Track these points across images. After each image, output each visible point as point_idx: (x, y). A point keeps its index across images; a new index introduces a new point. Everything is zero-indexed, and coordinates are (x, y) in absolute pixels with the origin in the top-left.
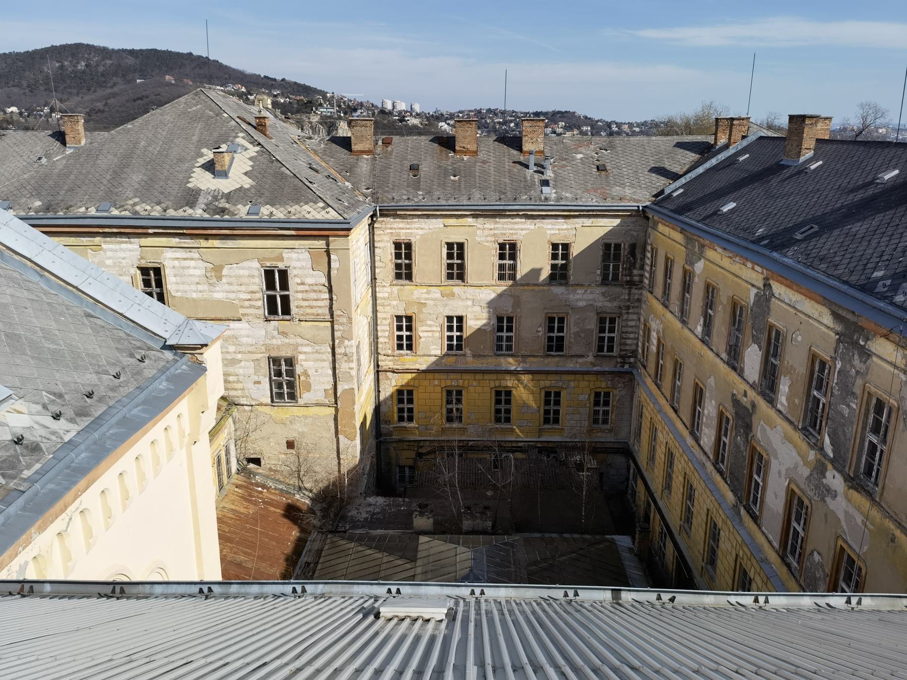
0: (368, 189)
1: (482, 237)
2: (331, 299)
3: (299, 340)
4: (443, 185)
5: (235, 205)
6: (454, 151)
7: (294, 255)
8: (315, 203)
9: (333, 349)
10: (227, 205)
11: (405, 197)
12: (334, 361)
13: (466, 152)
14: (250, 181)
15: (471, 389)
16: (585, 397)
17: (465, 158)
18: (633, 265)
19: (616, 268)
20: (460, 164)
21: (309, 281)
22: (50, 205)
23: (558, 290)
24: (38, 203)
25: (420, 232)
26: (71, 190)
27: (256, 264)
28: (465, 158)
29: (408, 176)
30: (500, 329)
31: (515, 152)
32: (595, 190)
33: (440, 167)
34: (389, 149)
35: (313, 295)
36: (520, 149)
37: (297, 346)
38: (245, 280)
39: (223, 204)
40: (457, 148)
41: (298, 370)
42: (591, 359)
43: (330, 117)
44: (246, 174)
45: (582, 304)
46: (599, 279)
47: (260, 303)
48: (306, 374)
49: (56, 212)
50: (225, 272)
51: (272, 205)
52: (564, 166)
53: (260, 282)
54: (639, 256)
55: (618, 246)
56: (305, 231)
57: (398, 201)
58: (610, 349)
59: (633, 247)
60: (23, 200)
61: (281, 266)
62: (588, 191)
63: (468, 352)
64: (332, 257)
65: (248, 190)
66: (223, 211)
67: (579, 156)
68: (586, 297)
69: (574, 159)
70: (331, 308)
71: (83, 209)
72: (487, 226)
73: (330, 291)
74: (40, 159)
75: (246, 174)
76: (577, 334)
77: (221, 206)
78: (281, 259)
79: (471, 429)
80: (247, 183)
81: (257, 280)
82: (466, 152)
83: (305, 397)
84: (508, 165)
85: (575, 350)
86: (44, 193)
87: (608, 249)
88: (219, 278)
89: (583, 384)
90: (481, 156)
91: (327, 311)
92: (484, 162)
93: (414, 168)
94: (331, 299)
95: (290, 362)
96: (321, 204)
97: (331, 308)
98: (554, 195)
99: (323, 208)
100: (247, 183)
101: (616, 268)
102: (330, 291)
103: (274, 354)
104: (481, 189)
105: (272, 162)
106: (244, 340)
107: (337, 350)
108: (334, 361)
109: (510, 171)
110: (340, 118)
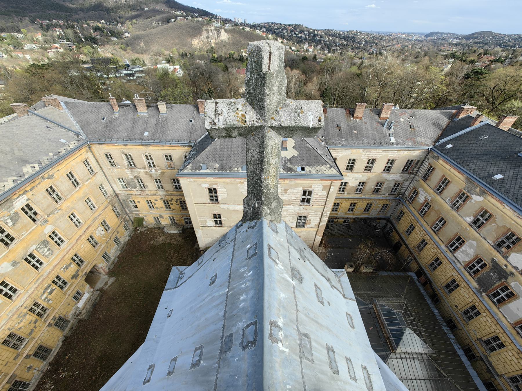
0: (322, 137)
1: (362, 155)
2: (326, 200)
3: (310, 211)
4: (351, 135)
5: (294, 166)
6: (353, 117)
7: (317, 186)
8: (326, 165)
9: (322, 213)
10: (291, 166)
11: (338, 142)
12: (321, 217)
13: (357, 118)
14: (296, 152)
15: (343, 203)
16: (380, 205)
17: (358, 120)
18: (415, 167)
19: (408, 167)
20: (356, 124)
21: (320, 194)
22: (222, 167)
23: (385, 175)
24: (217, 166)
25: (341, 155)
26: (228, 158)
27: (301, 189)
28: (358, 120)
29: (336, 130)
30: (359, 185)
31: (377, 117)
32: (411, 139)
33: (348, 125)
34: (327, 115)
35: (320, 198)
36: (379, 117)
37: (308, 213)
38: (296, 194)
39: (290, 166)
40: (355, 116)
41: (308, 219)
42: (387, 195)
43: (218, 27)
44: (293, 147)
45: (391, 179)
46: (401, 171)
47: (299, 200)
48: (310, 220)
49: (226, 171)
50: (288, 191)
51: (309, 166)
52: (397, 126)
53: (301, 194)
54: (419, 164)
55: (412, 161)
56: (322, 177)
57: (335, 145)
58: (394, 192)
59: (419, 161)
60: (211, 163)
61: (310, 189)
62: (408, 139)
63: (346, 192)
64: (332, 187)
65: (297, 157)
66: (290, 170)
67: (402, 120)
68: (394, 176)
69: (400, 122)
70: (326, 202)
71: (236, 169)
72: (367, 153)
73: (327, 197)
74: (191, 121)
75: (293, 147)
76: (385, 188)
77: (289, 166)
78: (311, 187)
79: (339, 213)
80: (296, 153)
81: (300, 194)
82: (357, 118)
83: (308, 226)
84: (375, 125)
85: (383, 192)
86: (218, 160)
87: (410, 162)
88: (286, 193)
89: (381, 202)
90: (364, 119)
91: (324, 203)
92: (365, 123)
93: (338, 126)
94: (326, 200)
95: (305, 217)
96: (328, 166)
97: (326, 202)
98: (395, 142)
99: (330, 168)
100: (296, 153)
101: (408, 167)
102: (327, 197)
103: (300, 215)
104: (367, 138)
105: (302, 140)
106: (290, 211)
107: (324, 214)
108: (321, 217)
109: (376, 128)
110: (221, 28)
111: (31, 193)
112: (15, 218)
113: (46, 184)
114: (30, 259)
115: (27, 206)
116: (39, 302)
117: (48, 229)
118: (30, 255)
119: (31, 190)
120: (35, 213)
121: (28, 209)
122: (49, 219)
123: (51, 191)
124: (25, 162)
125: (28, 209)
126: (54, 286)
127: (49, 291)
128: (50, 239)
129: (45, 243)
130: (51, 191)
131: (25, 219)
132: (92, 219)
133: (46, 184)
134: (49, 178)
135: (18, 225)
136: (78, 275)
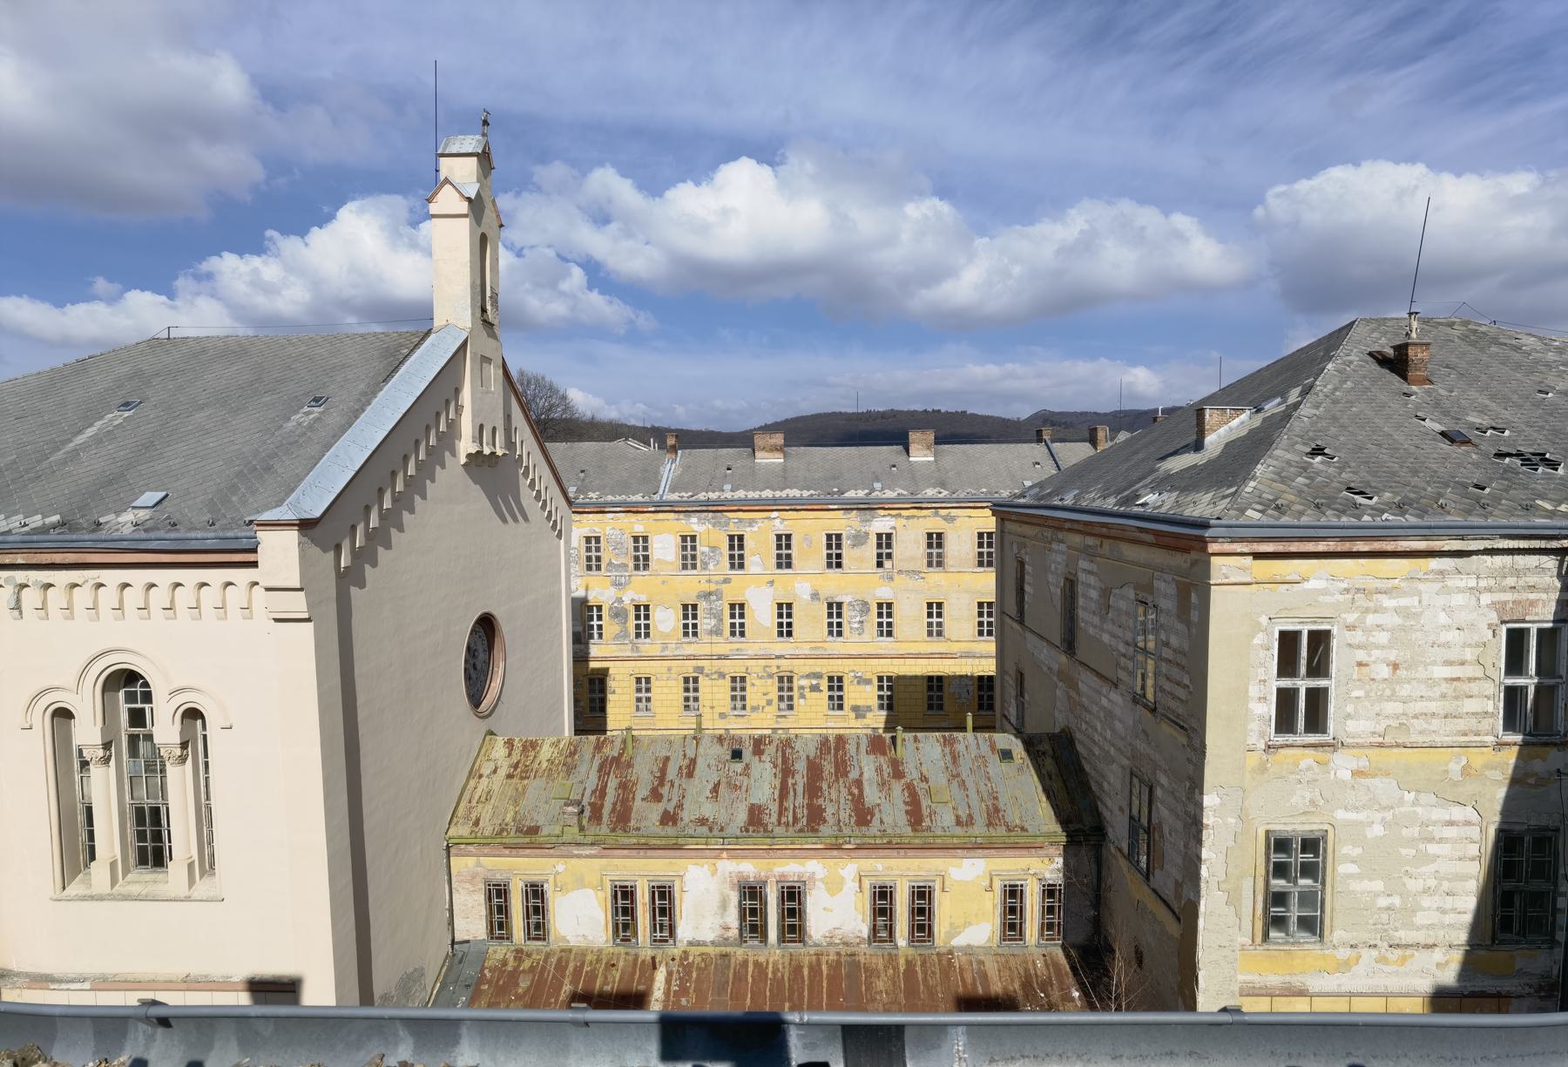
111: (904, 521)
112: (860, 539)
113: (934, 523)
114: (835, 608)
115: (889, 536)
116: (796, 684)
117: (884, 593)
118: (840, 605)
119: (908, 518)
120: (889, 556)
121: (885, 541)
122: (896, 577)
123: (935, 541)
124: (943, 485)
125: (885, 541)
126: (824, 684)
127: (814, 682)
128: (875, 610)
129: (865, 606)
130: (935, 541)
131: (871, 549)
132: (964, 647)
133: (934, 523)
134: (945, 518)
135: (857, 552)
136: (864, 717)
